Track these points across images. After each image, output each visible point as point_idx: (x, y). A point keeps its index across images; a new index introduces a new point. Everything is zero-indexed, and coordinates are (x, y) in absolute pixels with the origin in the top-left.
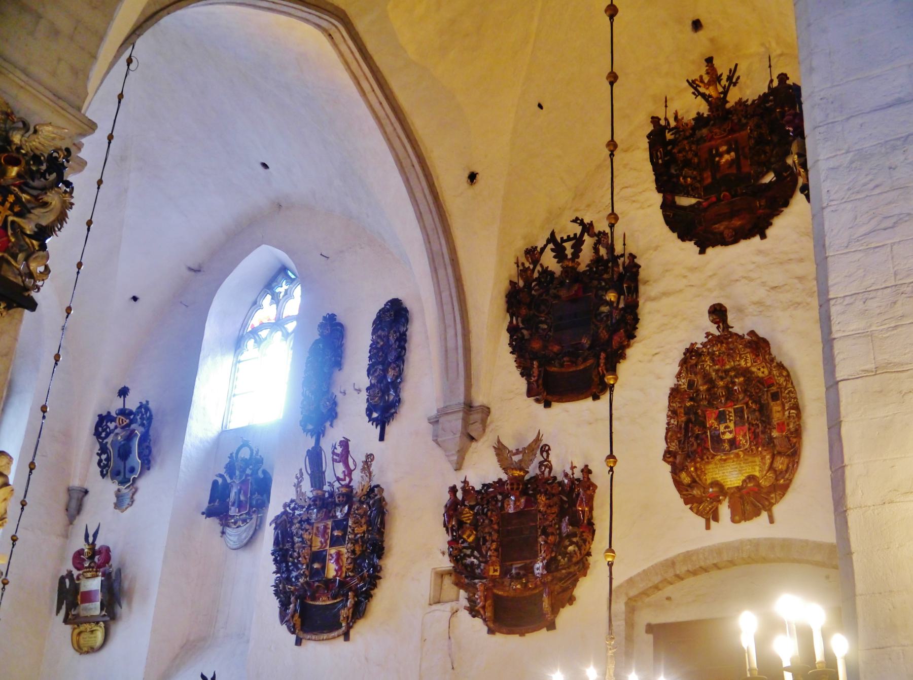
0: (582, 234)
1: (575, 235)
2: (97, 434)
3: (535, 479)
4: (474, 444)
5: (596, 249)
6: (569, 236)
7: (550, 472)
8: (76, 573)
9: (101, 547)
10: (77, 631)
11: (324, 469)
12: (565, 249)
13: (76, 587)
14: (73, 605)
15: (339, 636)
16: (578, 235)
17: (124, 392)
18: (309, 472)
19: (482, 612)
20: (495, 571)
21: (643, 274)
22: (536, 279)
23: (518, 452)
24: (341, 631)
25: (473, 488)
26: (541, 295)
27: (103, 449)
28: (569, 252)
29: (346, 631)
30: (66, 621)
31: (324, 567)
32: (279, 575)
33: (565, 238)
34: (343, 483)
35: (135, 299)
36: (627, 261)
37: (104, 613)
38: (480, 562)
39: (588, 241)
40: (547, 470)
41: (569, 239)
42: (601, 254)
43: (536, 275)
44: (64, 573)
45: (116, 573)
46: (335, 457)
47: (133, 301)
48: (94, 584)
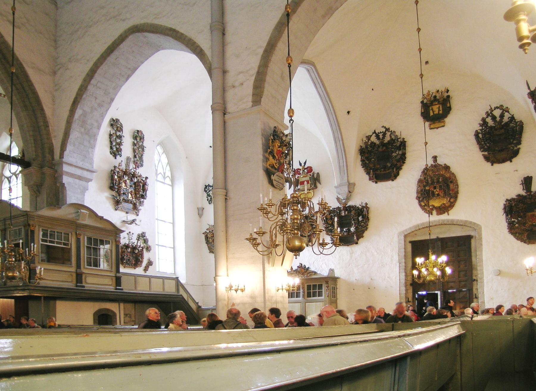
0: (385, 131)
1: (383, 131)
5: (391, 136)
6: (381, 132)
12: (379, 136)
16: (384, 132)
21: (407, 144)
22: (369, 145)
26: (371, 150)
28: (381, 137)
33: (379, 132)
36: (402, 140)
39: (388, 134)
41: (381, 133)
42: (392, 137)
43: (369, 144)
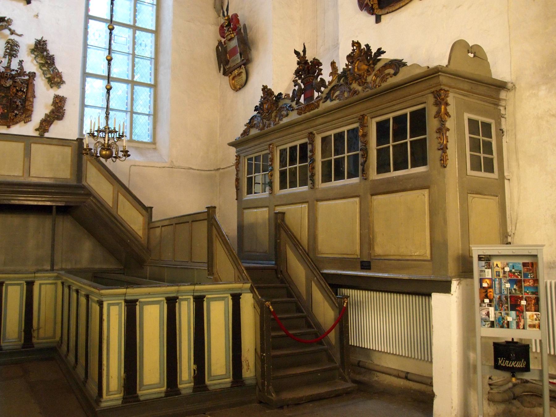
8: (223, 40)
9: (232, 16)
13: (225, 50)
14: (227, 62)
37: (242, 58)
44: (217, 44)
45: (243, 27)
48: (234, 43)
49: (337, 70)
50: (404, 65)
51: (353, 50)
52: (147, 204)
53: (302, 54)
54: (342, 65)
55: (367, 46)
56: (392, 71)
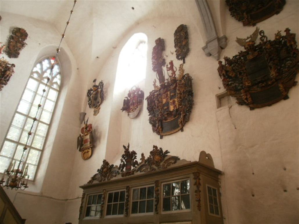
2: (88, 96)
3: (260, 44)
4: (223, 50)
7: (267, 39)
8: (82, 135)
9: (89, 125)
10: (83, 153)
11: (164, 75)
13: (82, 139)
14: (82, 145)
15: (179, 131)
17: (95, 81)
18: (158, 78)
19: (246, 101)
20: (248, 83)
23: (248, 38)
24: (179, 128)
25: (229, 58)
27: (90, 99)
29: (181, 127)
30: (80, 150)
31: (168, 108)
32: (151, 116)
34: (173, 77)
35: (98, 57)
37: (91, 145)
38: (239, 84)
40: (265, 38)
44: (79, 136)
45: (94, 131)
46: (168, 69)
47: (97, 58)
48: (88, 137)
49: (144, 158)
50: (179, 159)
51: (154, 150)
52: (23, 218)
53: (127, 148)
54: (147, 156)
55: (161, 148)
56: (173, 161)
